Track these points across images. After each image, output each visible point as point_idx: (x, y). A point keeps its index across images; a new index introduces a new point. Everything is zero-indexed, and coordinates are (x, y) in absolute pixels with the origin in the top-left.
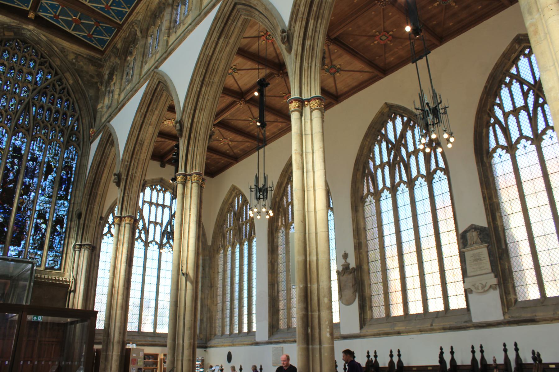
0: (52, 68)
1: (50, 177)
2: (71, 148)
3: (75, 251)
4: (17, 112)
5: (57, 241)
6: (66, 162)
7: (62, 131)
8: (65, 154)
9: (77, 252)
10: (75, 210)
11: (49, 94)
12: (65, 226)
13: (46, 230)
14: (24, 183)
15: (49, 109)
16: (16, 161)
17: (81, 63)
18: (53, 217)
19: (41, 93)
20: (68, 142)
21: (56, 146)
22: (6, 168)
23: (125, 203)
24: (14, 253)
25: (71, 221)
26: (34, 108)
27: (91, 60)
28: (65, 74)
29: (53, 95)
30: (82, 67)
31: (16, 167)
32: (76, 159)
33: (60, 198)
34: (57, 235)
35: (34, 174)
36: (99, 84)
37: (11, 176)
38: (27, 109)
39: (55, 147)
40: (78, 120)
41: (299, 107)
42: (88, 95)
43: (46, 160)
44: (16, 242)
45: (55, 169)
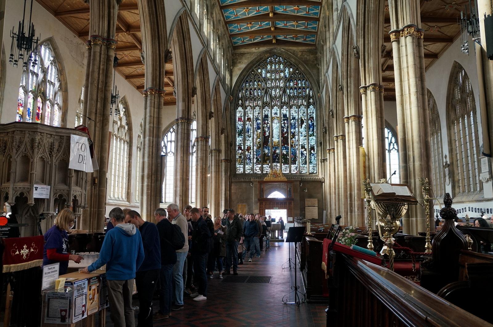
0: (291, 64)
1: (303, 126)
2: (311, 107)
3: (321, 162)
4: (280, 95)
5: (313, 159)
6: (310, 115)
7: (303, 98)
8: (309, 111)
9: (323, 163)
10: (319, 141)
11: (293, 80)
12: (315, 150)
13: (306, 154)
14: (291, 132)
15: (295, 88)
16: (286, 121)
17: (306, 56)
18: (309, 147)
19: (290, 80)
20: (308, 103)
21: (303, 108)
22: (282, 127)
23: (330, 142)
24: (294, 168)
25: (318, 147)
26: (288, 91)
27: (310, 52)
28: (299, 66)
29: (295, 80)
30: (306, 58)
31: (286, 125)
32: (315, 112)
33: (311, 136)
34: (313, 156)
35: (295, 126)
36: (317, 65)
37: (285, 130)
38: (284, 92)
39: (303, 108)
40: (311, 89)
41: (347, 121)
42: (313, 74)
43: (300, 117)
44: (294, 162)
45: (305, 121)
